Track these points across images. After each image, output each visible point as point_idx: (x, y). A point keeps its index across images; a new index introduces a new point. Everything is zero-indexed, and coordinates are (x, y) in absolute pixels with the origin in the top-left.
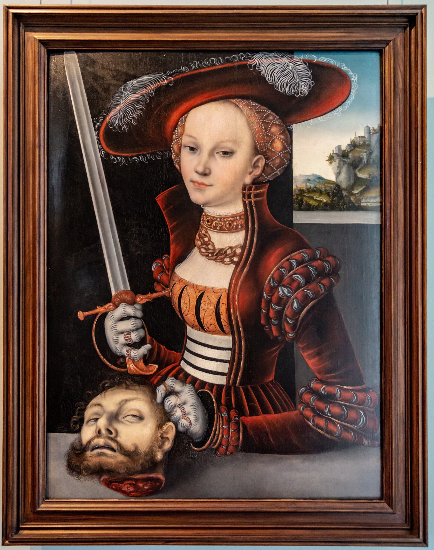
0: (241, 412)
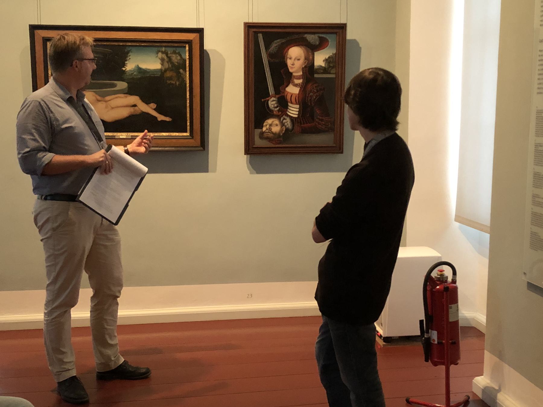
0: (301, 124)
